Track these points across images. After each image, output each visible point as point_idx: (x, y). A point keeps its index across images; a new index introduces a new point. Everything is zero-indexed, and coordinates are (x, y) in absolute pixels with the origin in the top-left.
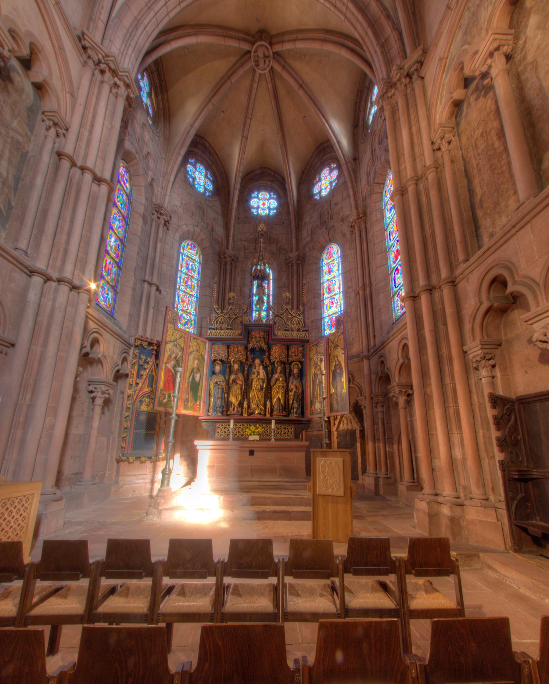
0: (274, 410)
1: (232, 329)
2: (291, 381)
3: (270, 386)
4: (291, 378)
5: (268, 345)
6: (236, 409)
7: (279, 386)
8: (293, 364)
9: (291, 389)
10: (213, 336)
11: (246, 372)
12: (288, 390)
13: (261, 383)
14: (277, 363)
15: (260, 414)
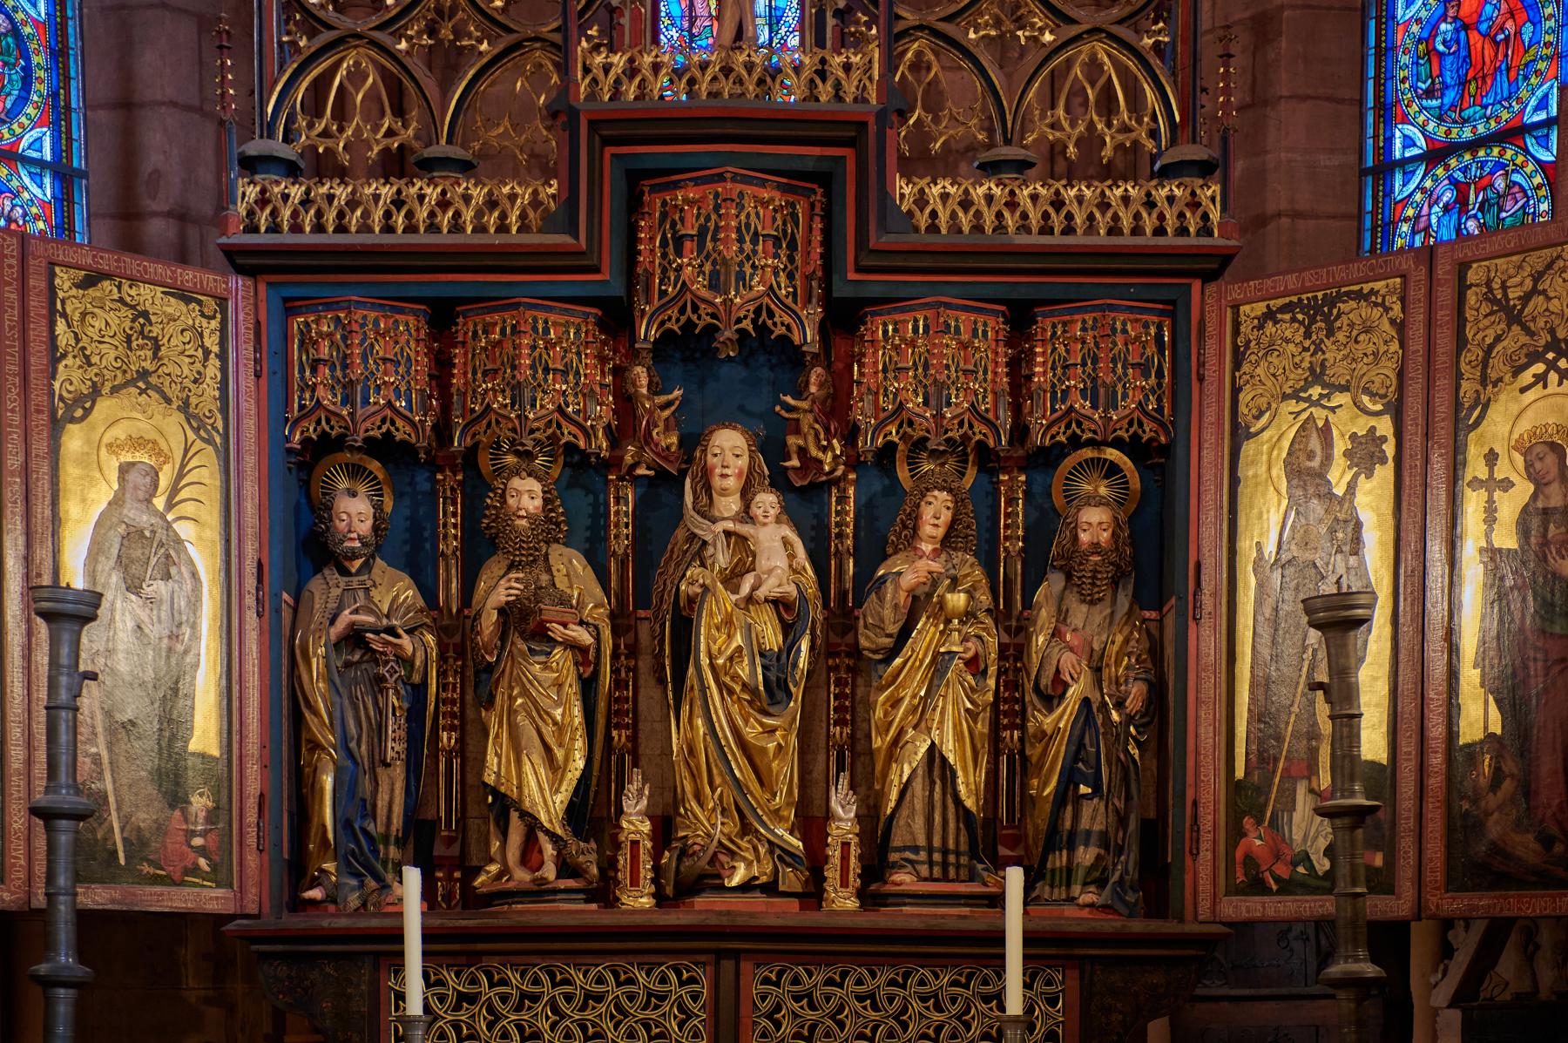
0: (894, 857)
1: (466, 167)
2: (1045, 616)
3: (855, 651)
4: (1053, 583)
5: (828, 301)
6: (549, 850)
7: (940, 663)
8: (1069, 462)
9: (1046, 681)
10: (286, 238)
11: (621, 539)
12: (1014, 685)
13: (772, 638)
14: (913, 463)
15: (771, 888)
